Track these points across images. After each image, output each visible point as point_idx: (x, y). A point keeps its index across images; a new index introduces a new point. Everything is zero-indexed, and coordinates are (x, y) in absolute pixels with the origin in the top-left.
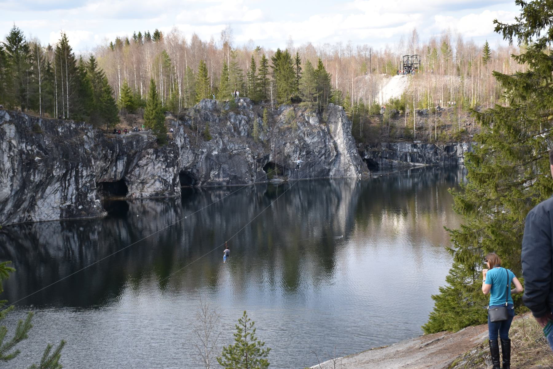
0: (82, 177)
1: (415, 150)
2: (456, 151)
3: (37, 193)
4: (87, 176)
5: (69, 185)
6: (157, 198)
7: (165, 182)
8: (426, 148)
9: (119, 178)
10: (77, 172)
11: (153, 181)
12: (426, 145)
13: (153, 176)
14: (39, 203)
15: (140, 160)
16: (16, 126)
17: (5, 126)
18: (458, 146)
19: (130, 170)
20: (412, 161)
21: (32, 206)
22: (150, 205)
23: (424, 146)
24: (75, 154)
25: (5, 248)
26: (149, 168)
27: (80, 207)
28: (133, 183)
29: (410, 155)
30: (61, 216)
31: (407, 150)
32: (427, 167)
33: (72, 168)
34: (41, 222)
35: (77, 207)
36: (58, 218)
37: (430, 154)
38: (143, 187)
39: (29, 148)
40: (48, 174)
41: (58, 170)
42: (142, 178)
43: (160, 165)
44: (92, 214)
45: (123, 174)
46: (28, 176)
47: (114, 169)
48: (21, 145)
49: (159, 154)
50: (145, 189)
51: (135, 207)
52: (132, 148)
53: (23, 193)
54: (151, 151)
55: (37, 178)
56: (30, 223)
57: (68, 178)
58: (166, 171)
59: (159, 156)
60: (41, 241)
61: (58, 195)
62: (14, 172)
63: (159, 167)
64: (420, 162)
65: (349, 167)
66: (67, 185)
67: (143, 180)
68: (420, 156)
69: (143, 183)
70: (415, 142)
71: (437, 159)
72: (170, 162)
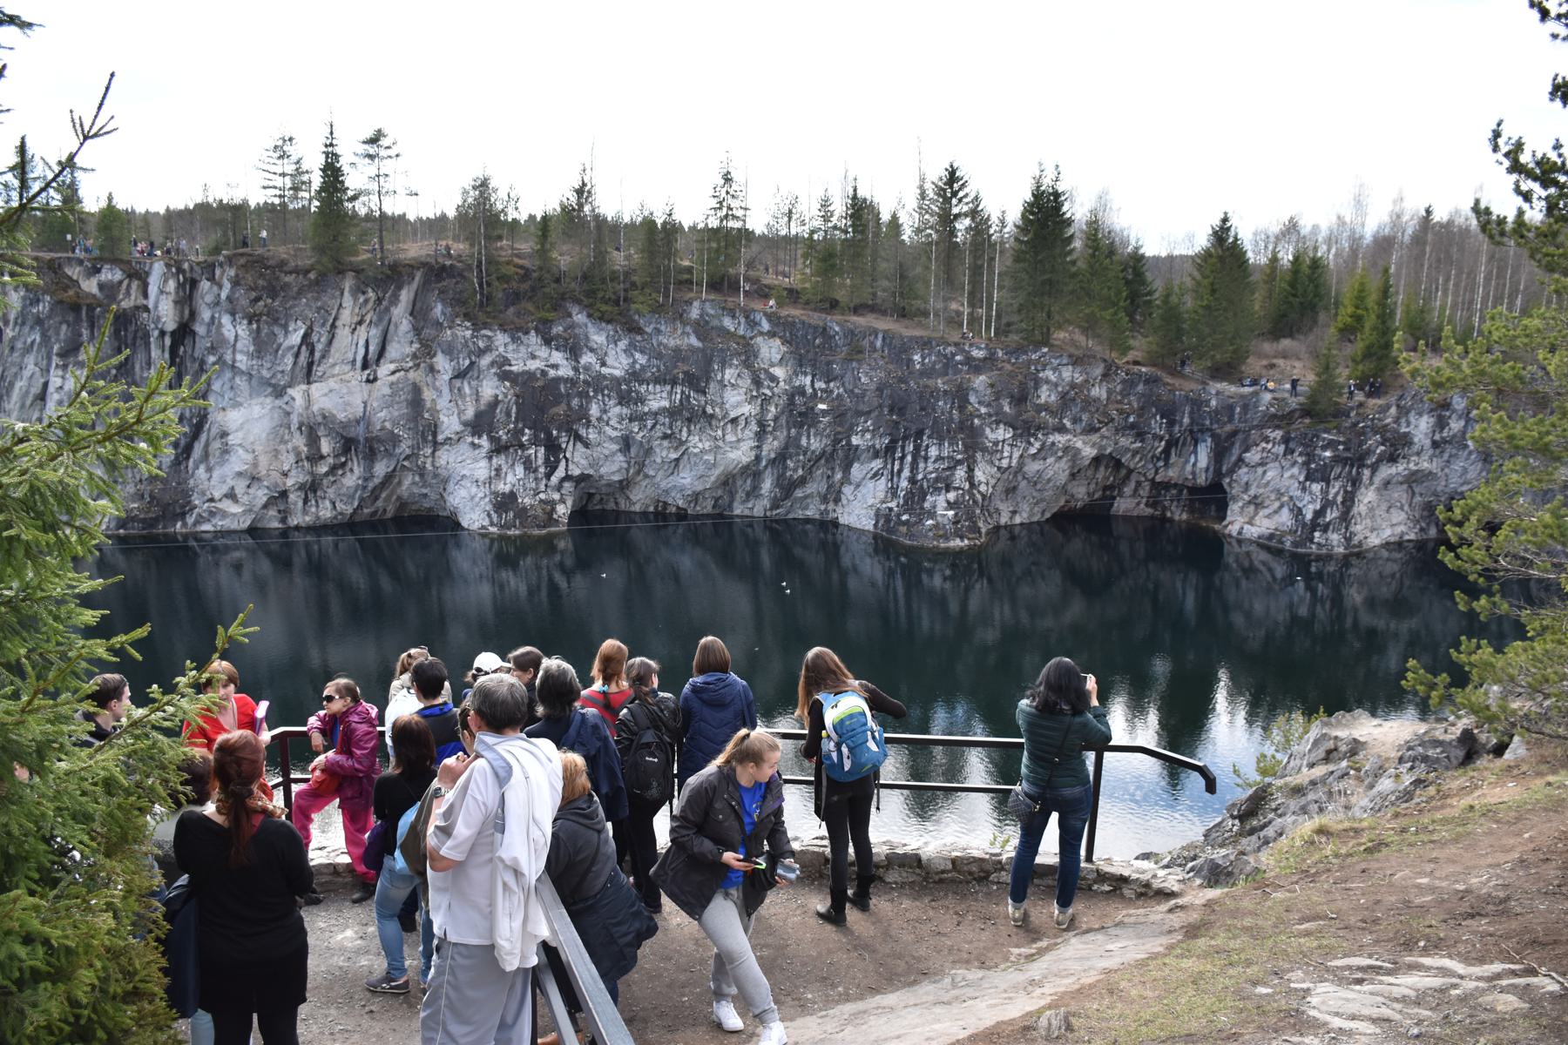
0: (926, 459)
3: (833, 469)
4: (939, 458)
5: (900, 471)
6: (1270, 544)
7: (1298, 513)
9: (1202, 480)
10: (917, 448)
11: (1277, 504)
13: (1279, 494)
14: (847, 490)
15: (1247, 450)
16: (785, 342)
17: (759, 339)
19: (1224, 469)
21: (833, 495)
22: (1260, 556)
24: (922, 409)
25: (755, 555)
26: (1270, 475)
27: (904, 518)
28: (1235, 499)
30: (876, 525)
33: (905, 438)
34: (850, 528)
35: (899, 515)
36: (871, 528)
38: (1256, 514)
39: (820, 385)
40: (836, 441)
41: (868, 436)
42: (1252, 492)
43: (1295, 470)
44: (911, 536)
45: (1210, 475)
46: (799, 435)
47: (1192, 460)
48: (801, 377)
49: (1292, 445)
50: (1257, 520)
51: (1231, 554)
52: (1231, 419)
53: (785, 468)
54: (1278, 434)
55: (816, 444)
56: (835, 524)
57: (898, 454)
58: (1304, 489)
59: (1293, 452)
60: (846, 561)
61: (882, 484)
62: (762, 424)
63: (1292, 476)
66: (896, 468)
67: (1255, 497)
69: (1257, 503)
72: (1316, 470)
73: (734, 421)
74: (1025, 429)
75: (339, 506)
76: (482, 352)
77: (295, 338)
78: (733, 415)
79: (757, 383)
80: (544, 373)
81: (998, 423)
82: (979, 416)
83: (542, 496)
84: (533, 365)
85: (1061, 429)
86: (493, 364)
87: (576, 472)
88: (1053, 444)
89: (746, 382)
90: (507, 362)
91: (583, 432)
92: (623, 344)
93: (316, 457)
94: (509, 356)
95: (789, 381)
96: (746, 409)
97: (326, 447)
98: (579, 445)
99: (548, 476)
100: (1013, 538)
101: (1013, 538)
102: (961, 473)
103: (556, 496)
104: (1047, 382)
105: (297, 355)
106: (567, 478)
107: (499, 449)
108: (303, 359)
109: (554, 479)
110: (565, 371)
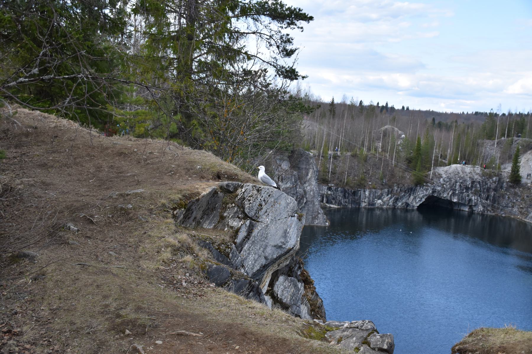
1: (329, 192)
2: (360, 196)
8: (338, 191)
12: (338, 188)
18: (362, 192)
20: (327, 202)
23: (336, 190)
29: (326, 197)
31: (323, 193)
32: (338, 208)
37: (340, 196)
64: (333, 204)
65: (317, 216)
68: (333, 199)
70: (330, 185)
71: (346, 202)
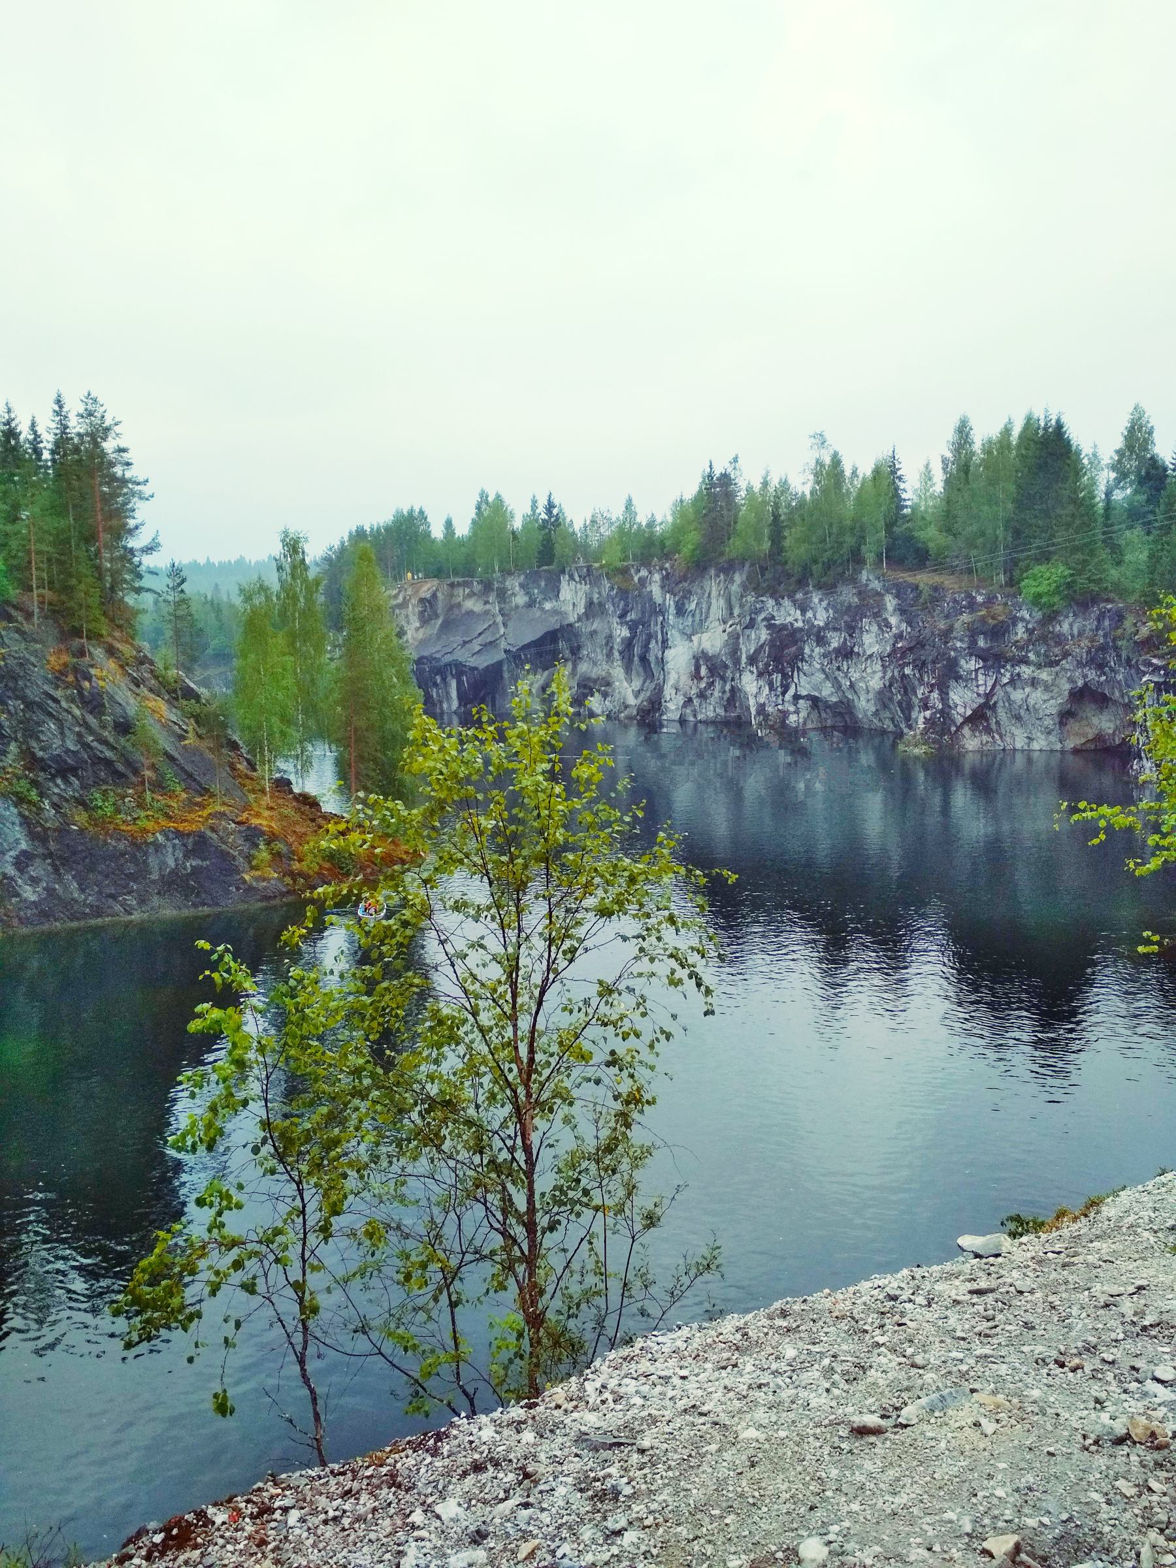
73: (871, 656)
74: (993, 660)
75: (718, 710)
76: (758, 612)
77: (693, 606)
78: (869, 653)
79: (880, 628)
80: (792, 624)
81: (971, 655)
82: (955, 649)
83: (780, 707)
84: (789, 619)
85: (1025, 661)
86: (765, 619)
87: (804, 693)
88: (1018, 675)
89: (875, 628)
90: (773, 618)
91: (800, 664)
92: (824, 604)
93: (696, 676)
94: (775, 614)
95: (898, 627)
96: (875, 649)
97: (703, 671)
98: (801, 674)
99: (784, 694)
100: (1030, 761)
101: (1030, 761)
102: (935, 695)
103: (792, 709)
104: (1023, 619)
105: (693, 616)
106: (797, 697)
107: (760, 675)
108: (697, 618)
109: (788, 696)
110: (800, 624)
